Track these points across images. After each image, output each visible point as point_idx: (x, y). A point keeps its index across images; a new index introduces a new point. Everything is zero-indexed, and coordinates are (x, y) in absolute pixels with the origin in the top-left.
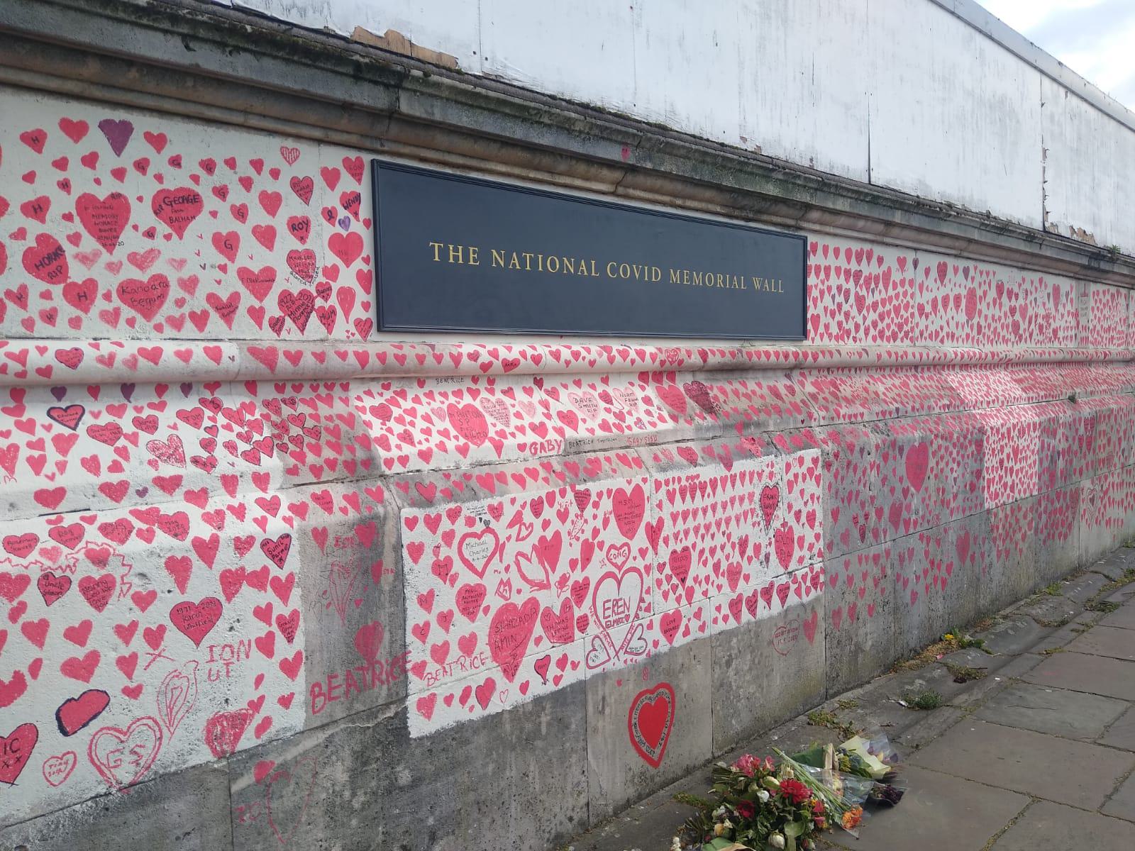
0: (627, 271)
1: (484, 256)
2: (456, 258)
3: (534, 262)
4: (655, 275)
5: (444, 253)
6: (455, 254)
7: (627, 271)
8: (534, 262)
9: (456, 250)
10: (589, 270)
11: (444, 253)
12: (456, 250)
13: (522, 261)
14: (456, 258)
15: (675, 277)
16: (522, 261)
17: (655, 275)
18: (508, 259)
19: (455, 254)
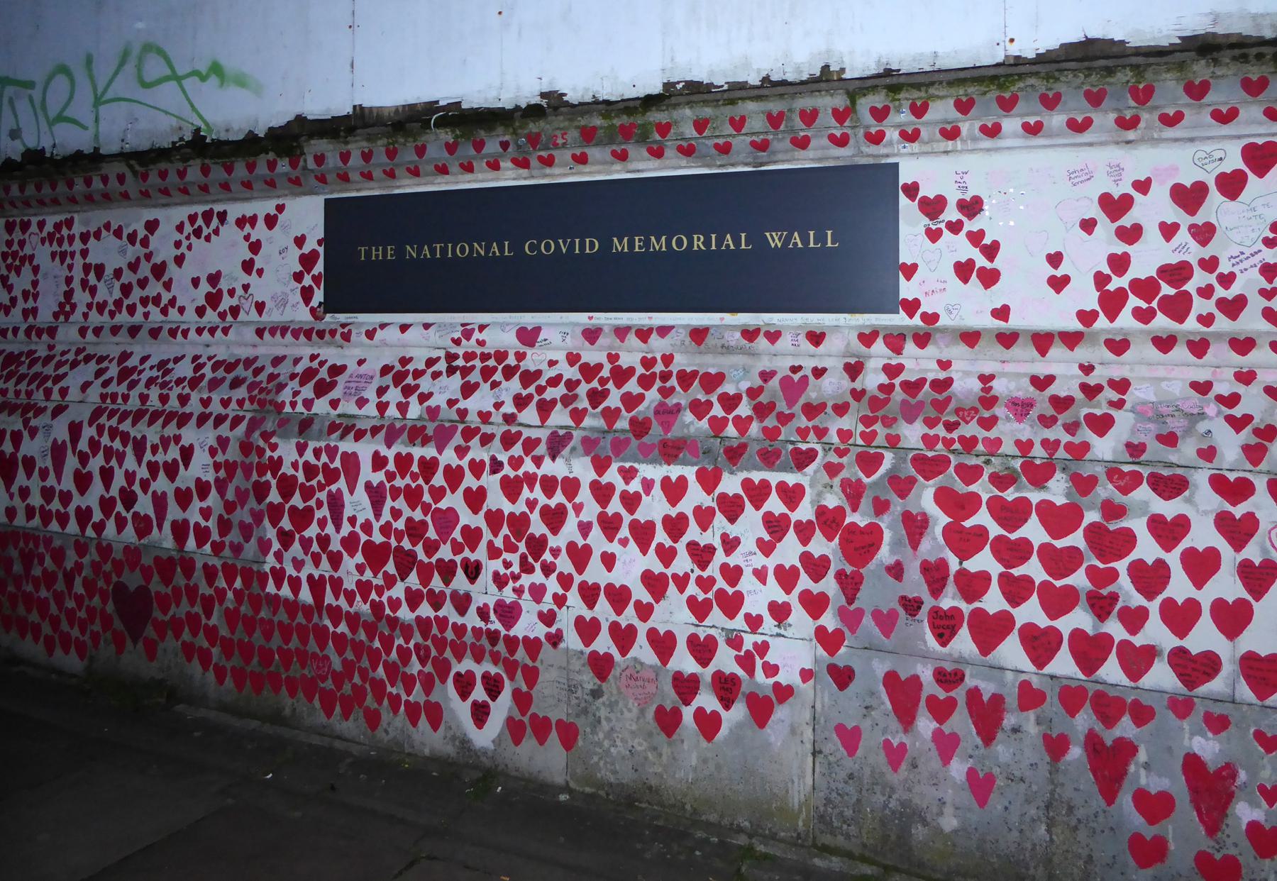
0: (548, 247)
1: (400, 252)
2: (377, 256)
3: (444, 251)
4: (592, 246)
5: (368, 254)
6: (377, 253)
7: (548, 247)
8: (444, 251)
9: (377, 250)
10: (501, 249)
11: (368, 254)
12: (377, 250)
13: (433, 251)
14: (377, 256)
15: (620, 245)
16: (433, 251)
17: (592, 246)
18: (419, 252)
19: (377, 253)
